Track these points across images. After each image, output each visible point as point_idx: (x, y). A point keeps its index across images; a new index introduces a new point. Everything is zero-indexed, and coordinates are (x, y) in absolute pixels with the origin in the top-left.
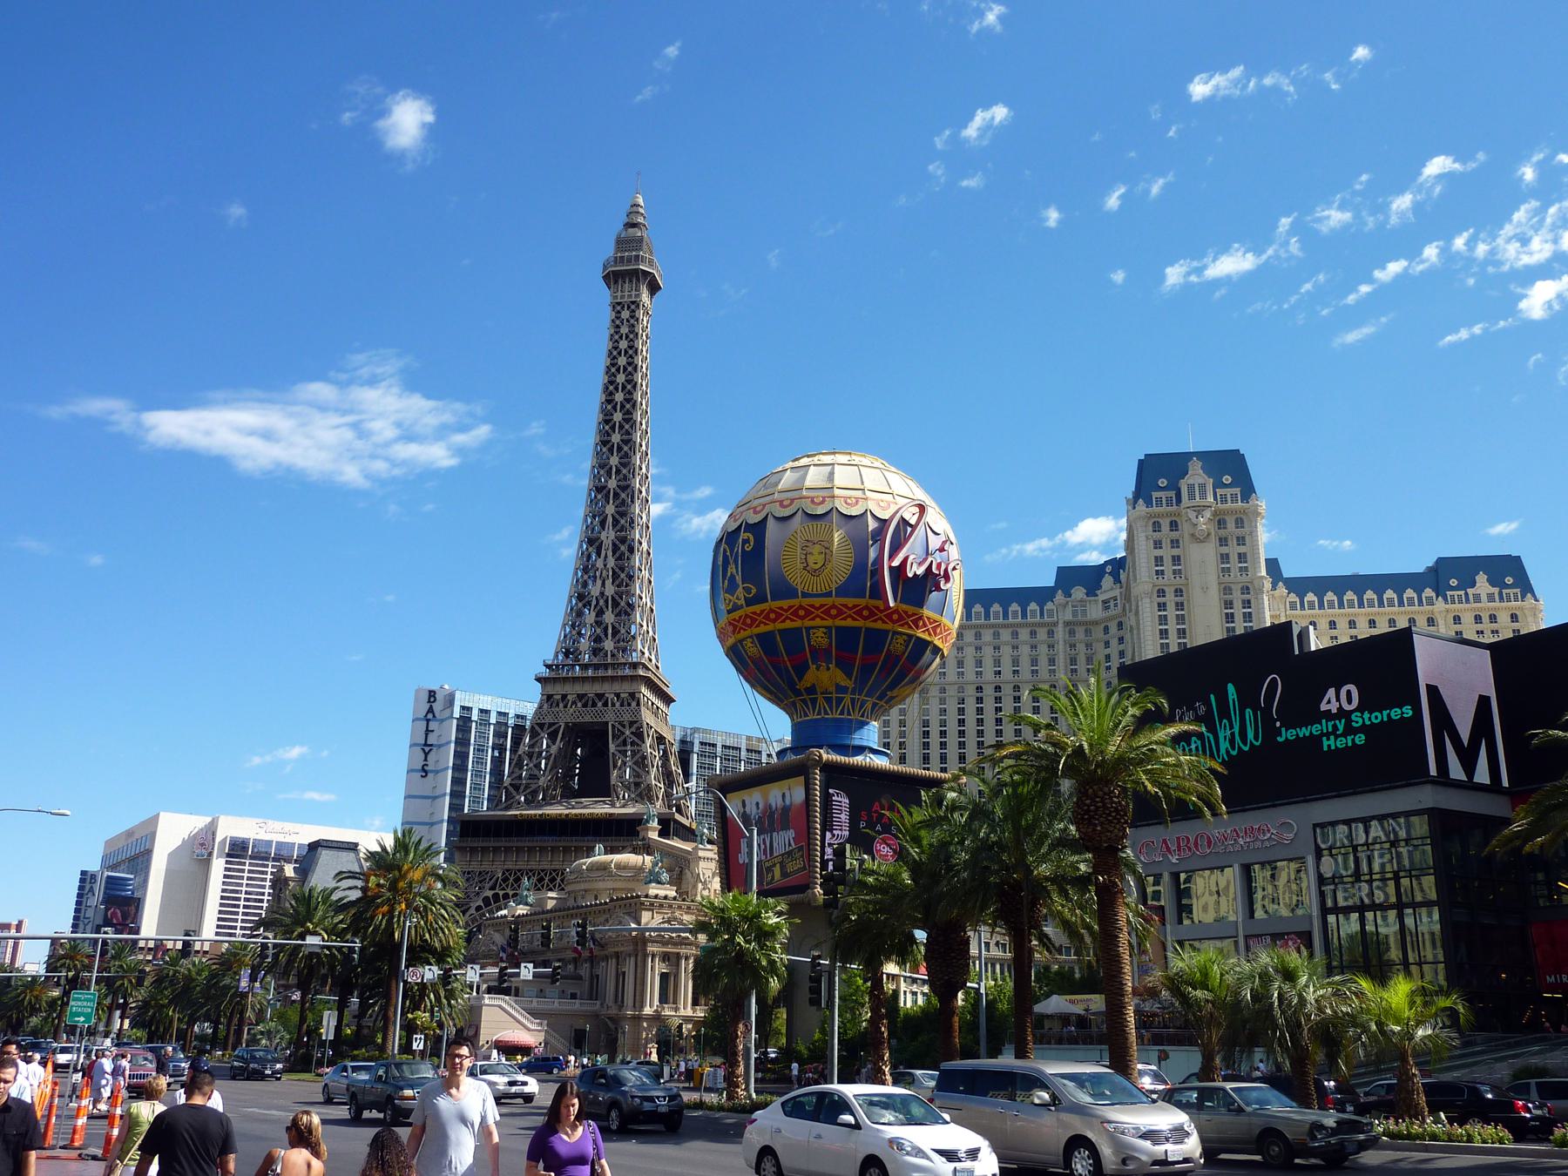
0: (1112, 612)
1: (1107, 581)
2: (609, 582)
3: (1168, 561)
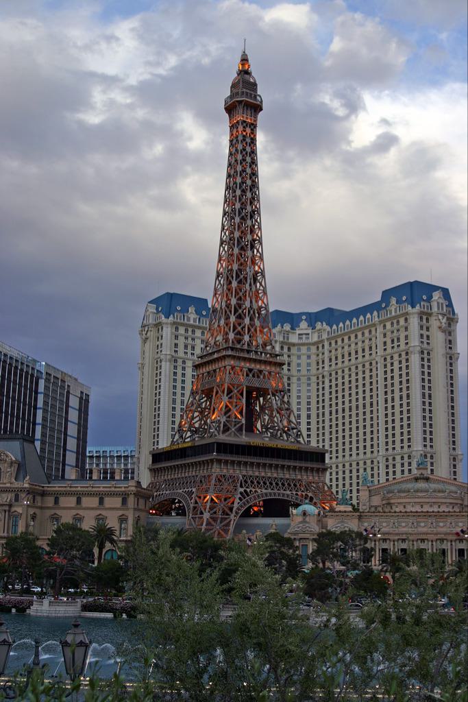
0: (304, 340)
1: (304, 325)
2: (254, 301)
3: (425, 337)
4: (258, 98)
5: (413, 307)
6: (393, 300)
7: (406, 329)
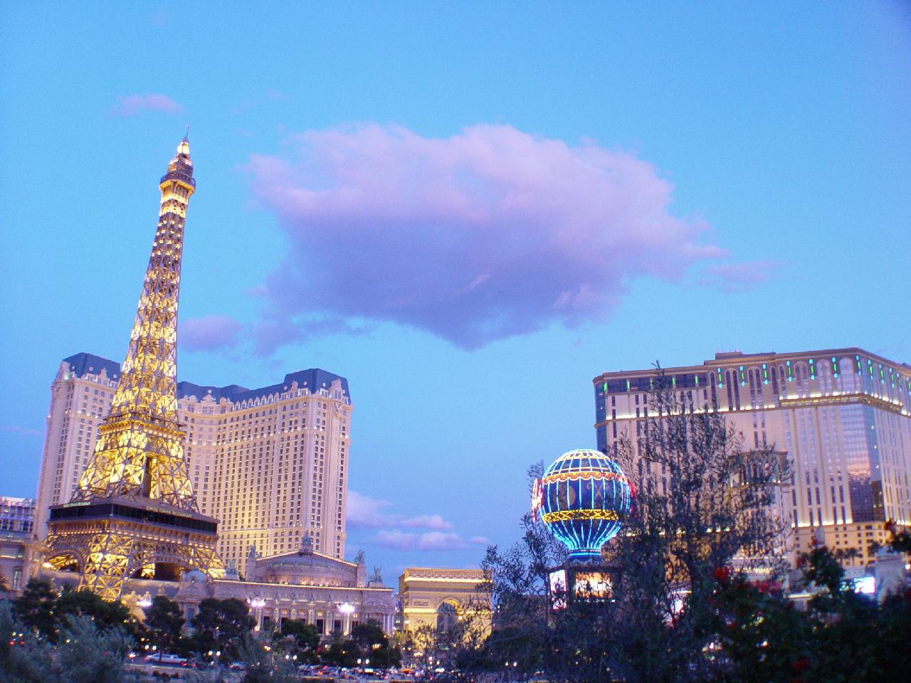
3: (321, 422)
4: (192, 181)
5: (313, 392)
6: (295, 384)
7: (304, 412)
